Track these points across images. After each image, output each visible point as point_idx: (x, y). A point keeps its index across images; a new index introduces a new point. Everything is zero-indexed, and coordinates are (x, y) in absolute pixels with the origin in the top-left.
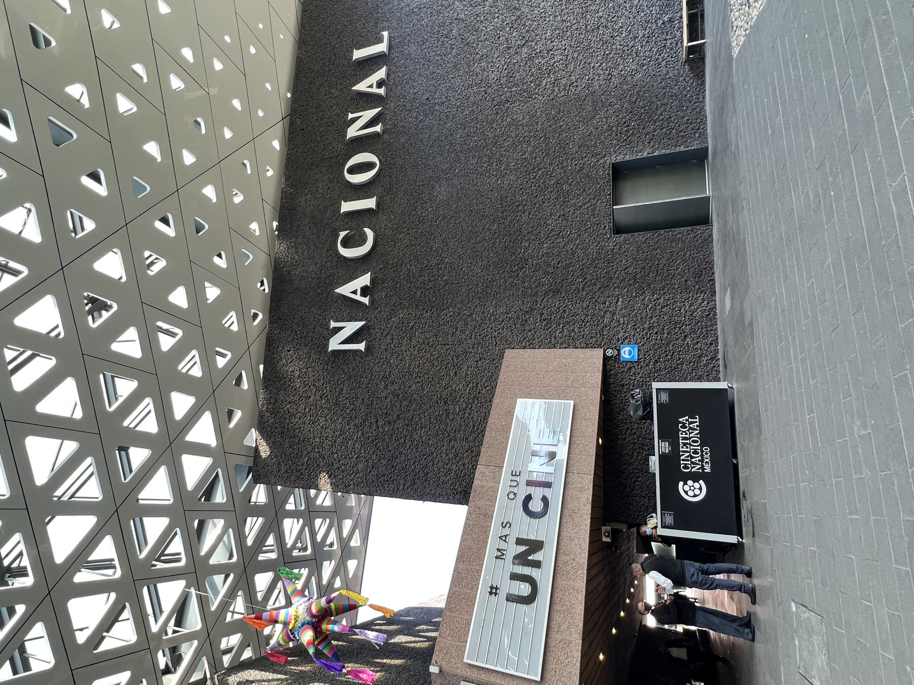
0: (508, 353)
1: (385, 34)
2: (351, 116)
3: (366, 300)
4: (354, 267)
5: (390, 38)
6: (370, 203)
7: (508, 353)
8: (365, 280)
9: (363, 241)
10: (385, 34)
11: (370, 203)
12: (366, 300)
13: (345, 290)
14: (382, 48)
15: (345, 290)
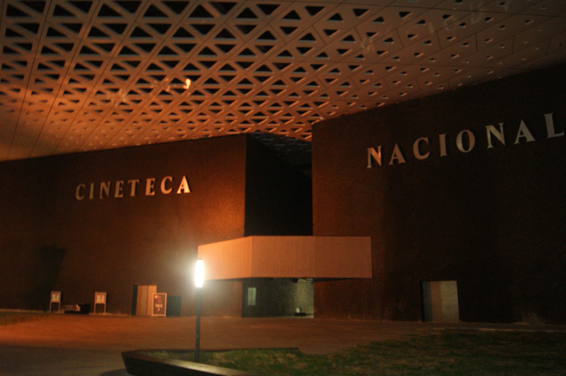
0: (370, 238)
1: (562, 134)
2: (501, 125)
3: (391, 163)
4: (407, 152)
5: (560, 138)
6: (443, 152)
7: (370, 238)
8: (401, 160)
9: (422, 153)
10: (562, 134)
11: (443, 153)
12: (391, 163)
13: (397, 150)
14: (551, 132)
15: (397, 150)
